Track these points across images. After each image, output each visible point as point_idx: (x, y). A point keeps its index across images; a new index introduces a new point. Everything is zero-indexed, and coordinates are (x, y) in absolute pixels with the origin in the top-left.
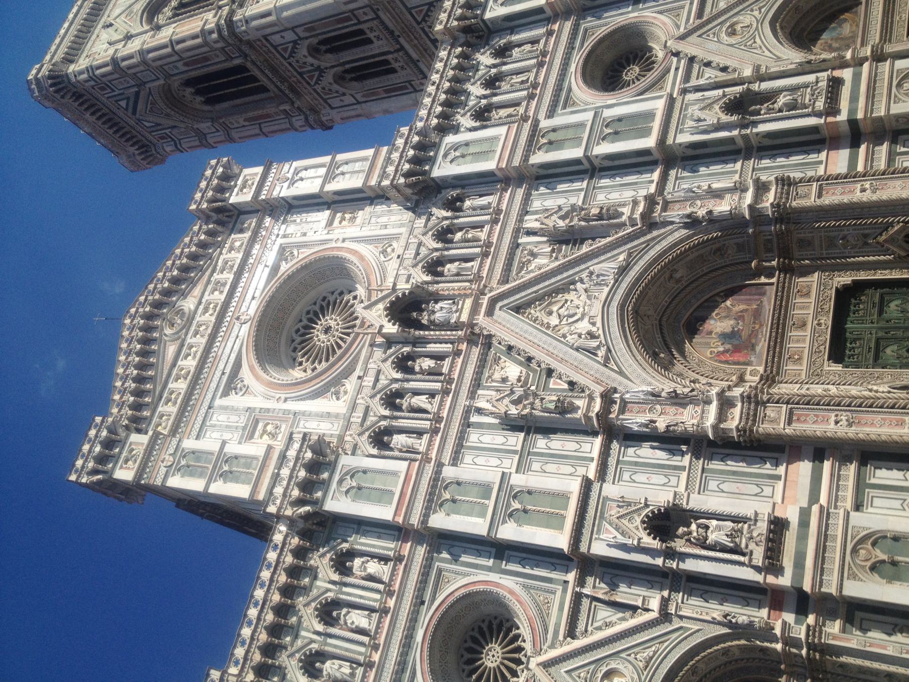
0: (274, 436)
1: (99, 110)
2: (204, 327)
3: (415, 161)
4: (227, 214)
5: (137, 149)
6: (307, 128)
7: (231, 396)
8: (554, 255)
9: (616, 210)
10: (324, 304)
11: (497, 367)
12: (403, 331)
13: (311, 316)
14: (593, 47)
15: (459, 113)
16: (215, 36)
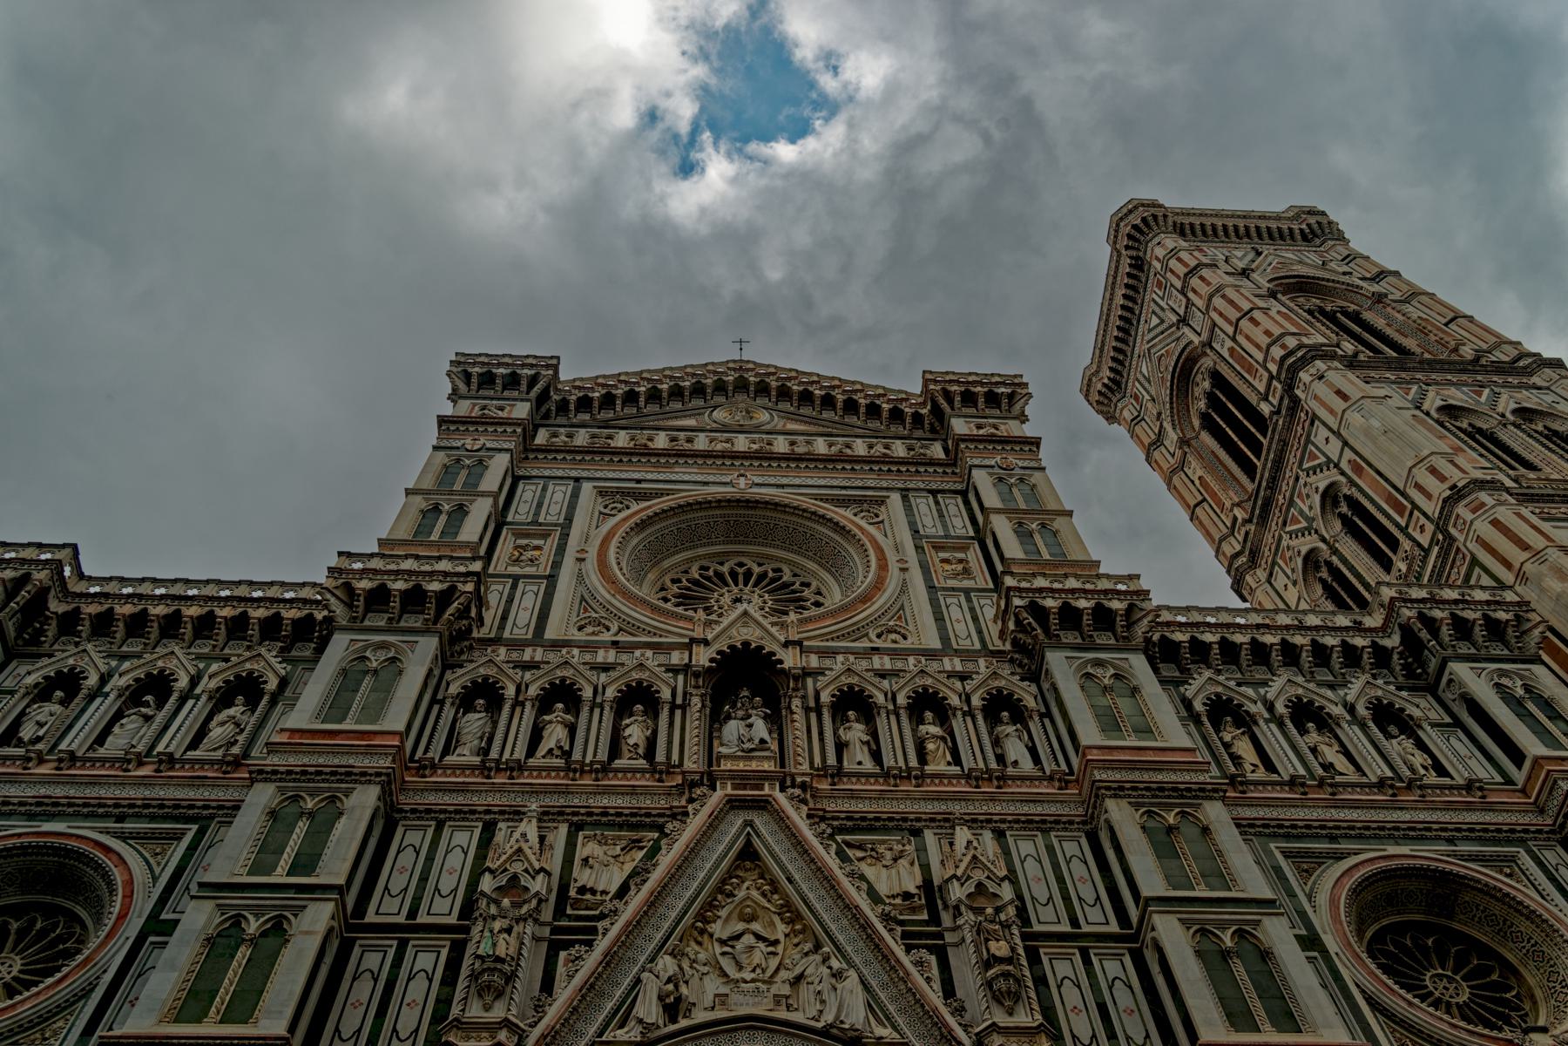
0: (517, 560)
1: (1134, 300)
2: (729, 445)
3: (1070, 616)
4: (936, 424)
5: (1109, 378)
6: (1226, 564)
7: (600, 500)
8: (898, 901)
9: (1016, 997)
10: (797, 586)
11: (618, 848)
12: (696, 675)
13: (771, 574)
14: (1473, 879)
15: (1219, 672)
16: (1282, 353)
